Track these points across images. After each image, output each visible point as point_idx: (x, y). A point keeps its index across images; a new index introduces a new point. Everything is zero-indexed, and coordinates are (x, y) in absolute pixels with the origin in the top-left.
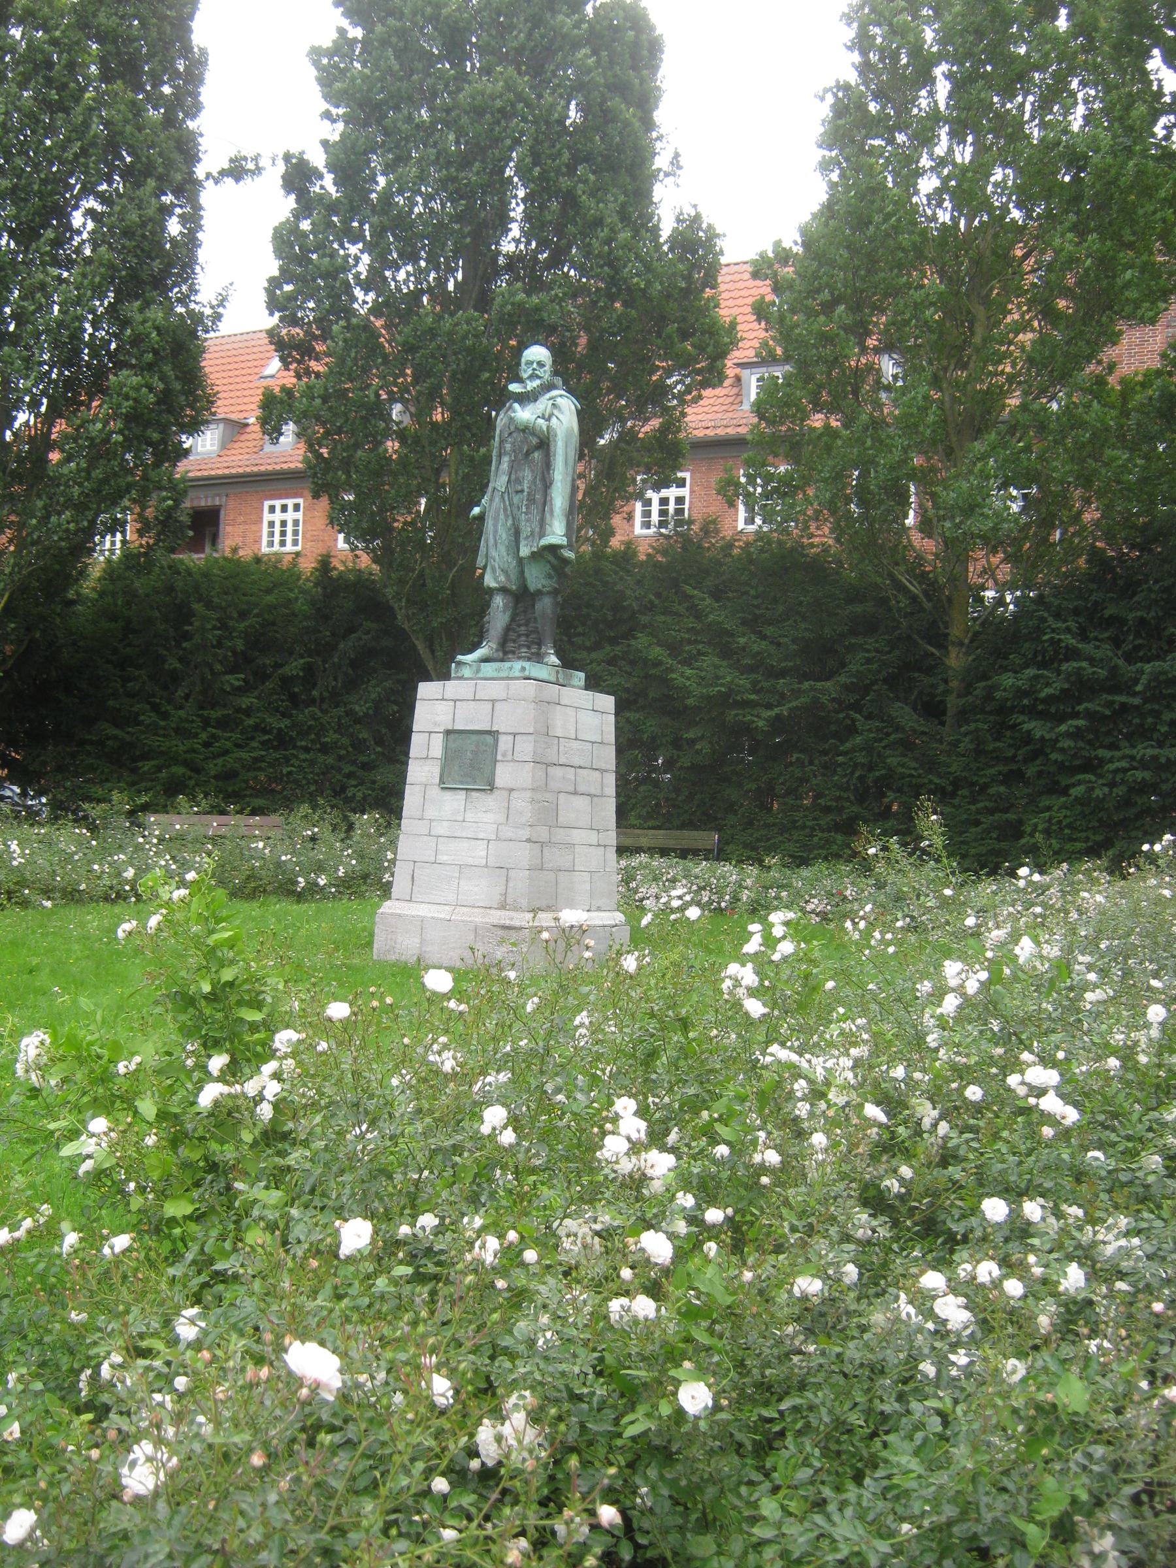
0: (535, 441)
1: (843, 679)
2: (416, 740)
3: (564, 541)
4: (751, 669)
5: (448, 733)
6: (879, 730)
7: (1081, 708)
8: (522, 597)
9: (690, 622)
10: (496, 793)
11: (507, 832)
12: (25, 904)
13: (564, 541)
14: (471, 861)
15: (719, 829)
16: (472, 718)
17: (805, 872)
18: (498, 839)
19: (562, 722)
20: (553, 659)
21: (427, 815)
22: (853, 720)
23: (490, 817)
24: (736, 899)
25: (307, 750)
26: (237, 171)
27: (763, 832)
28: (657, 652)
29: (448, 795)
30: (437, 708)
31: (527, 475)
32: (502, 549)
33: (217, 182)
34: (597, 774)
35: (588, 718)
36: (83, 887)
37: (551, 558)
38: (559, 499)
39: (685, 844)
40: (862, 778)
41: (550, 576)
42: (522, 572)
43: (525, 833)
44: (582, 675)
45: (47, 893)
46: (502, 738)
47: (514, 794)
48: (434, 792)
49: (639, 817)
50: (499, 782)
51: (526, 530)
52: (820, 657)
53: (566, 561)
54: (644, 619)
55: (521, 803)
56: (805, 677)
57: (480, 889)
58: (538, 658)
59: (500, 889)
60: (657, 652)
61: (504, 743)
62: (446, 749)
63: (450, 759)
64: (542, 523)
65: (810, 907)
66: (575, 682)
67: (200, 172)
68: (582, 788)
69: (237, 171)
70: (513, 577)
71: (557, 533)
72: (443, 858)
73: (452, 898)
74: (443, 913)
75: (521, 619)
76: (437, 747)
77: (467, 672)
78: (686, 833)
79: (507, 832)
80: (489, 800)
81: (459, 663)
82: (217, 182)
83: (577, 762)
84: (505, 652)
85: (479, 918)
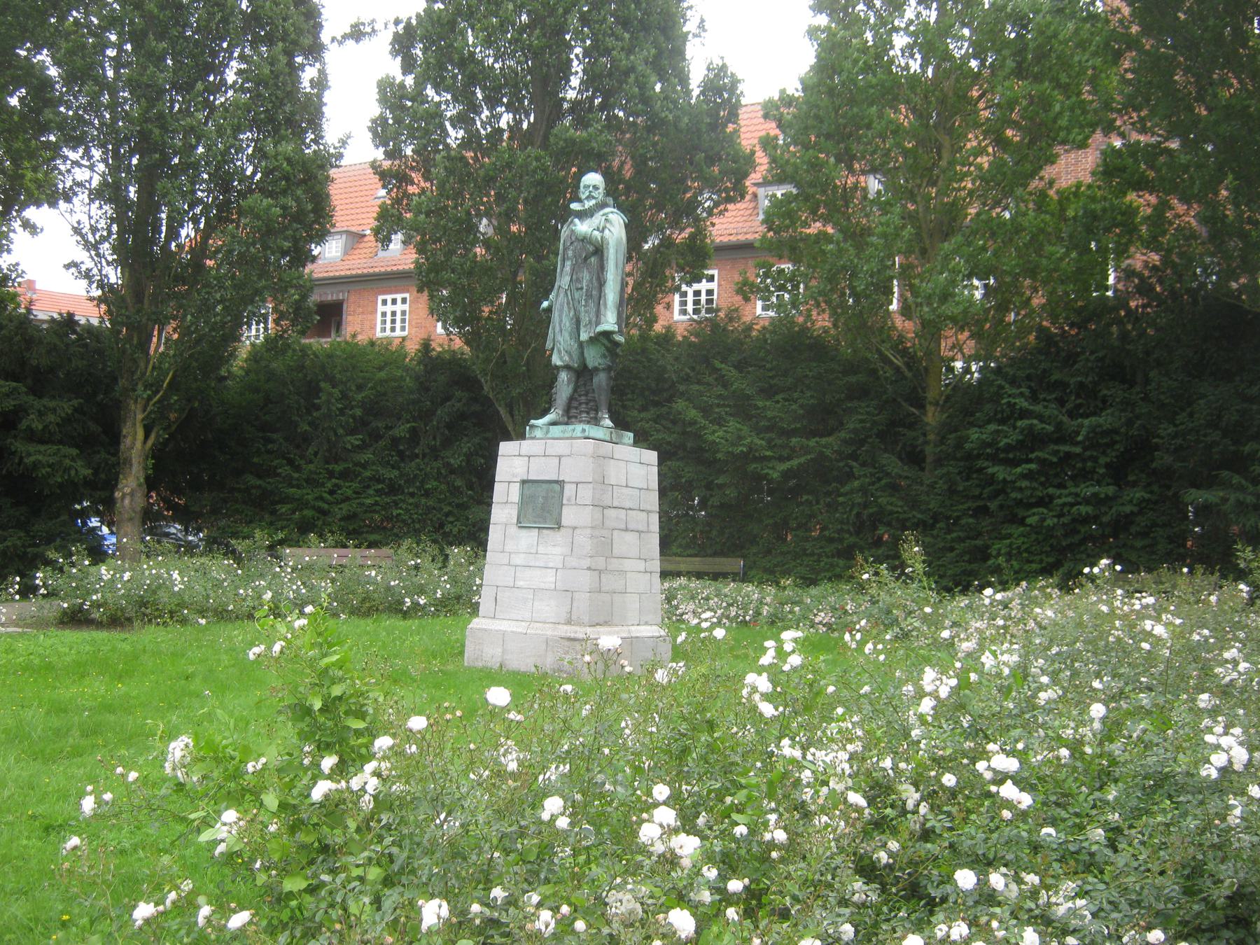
0: (591, 249)
1: (843, 435)
2: (499, 490)
3: (616, 328)
4: (769, 429)
5: (524, 482)
6: (872, 475)
7: (1032, 456)
8: (582, 373)
9: (719, 390)
11: (573, 562)
12: (184, 621)
13: (616, 328)
14: (542, 586)
15: (744, 557)
16: (543, 470)
17: (814, 591)
18: (564, 567)
19: (615, 473)
20: (608, 423)
21: (507, 548)
22: (851, 468)
23: (558, 550)
24: (758, 613)
25: (412, 495)
26: (357, 33)
27: (779, 559)
28: (693, 413)
29: (524, 533)
30: (515, 462)
31: (586, 276)
32: (566, 335)
33: (340, 43)
34: (645, 514)
35: (637, 468)
36: (231, 607)
37: (606, 342)
38: (611, 294)
39: (717, 569)
40: (858, 515)
41: (604, 356)
42: (582, 353)
43: (586, 563)
44: (631, 435)
45: (202, 612)
46: (567, 487)
47: (578, 532)
48: (513, 530)
49: (680, 546)
50: (563, 523)
51: (585, 319)
52: (822, 419)
53: (617, 344)
54: (682, 388)
55: (583, 539)
56: (814, 434)
57: (549, 609)
58: (596, 421)
60: (693, 413)
61: (569, 490)
62: (522, 495)
63: (525, 502)
64: (598, 314)
65: (817, 620)
66: (626, 440)
67: (325, 37)
68: (631, 526)
69: (357, 33)
70: (575, 357)
71: (609, 322)
72: (520, 583)
73: (527, 615)
74: (520, 628)
75: (582, 390)
76: (515, 493)
77: (538, 433)
78: (717, 560)
79: (573, 562)
80: (558, 537)
81: (532, 427)
82: (340, 43)
83: (628, 505)
84: (569, 416)
85: (549, 631)
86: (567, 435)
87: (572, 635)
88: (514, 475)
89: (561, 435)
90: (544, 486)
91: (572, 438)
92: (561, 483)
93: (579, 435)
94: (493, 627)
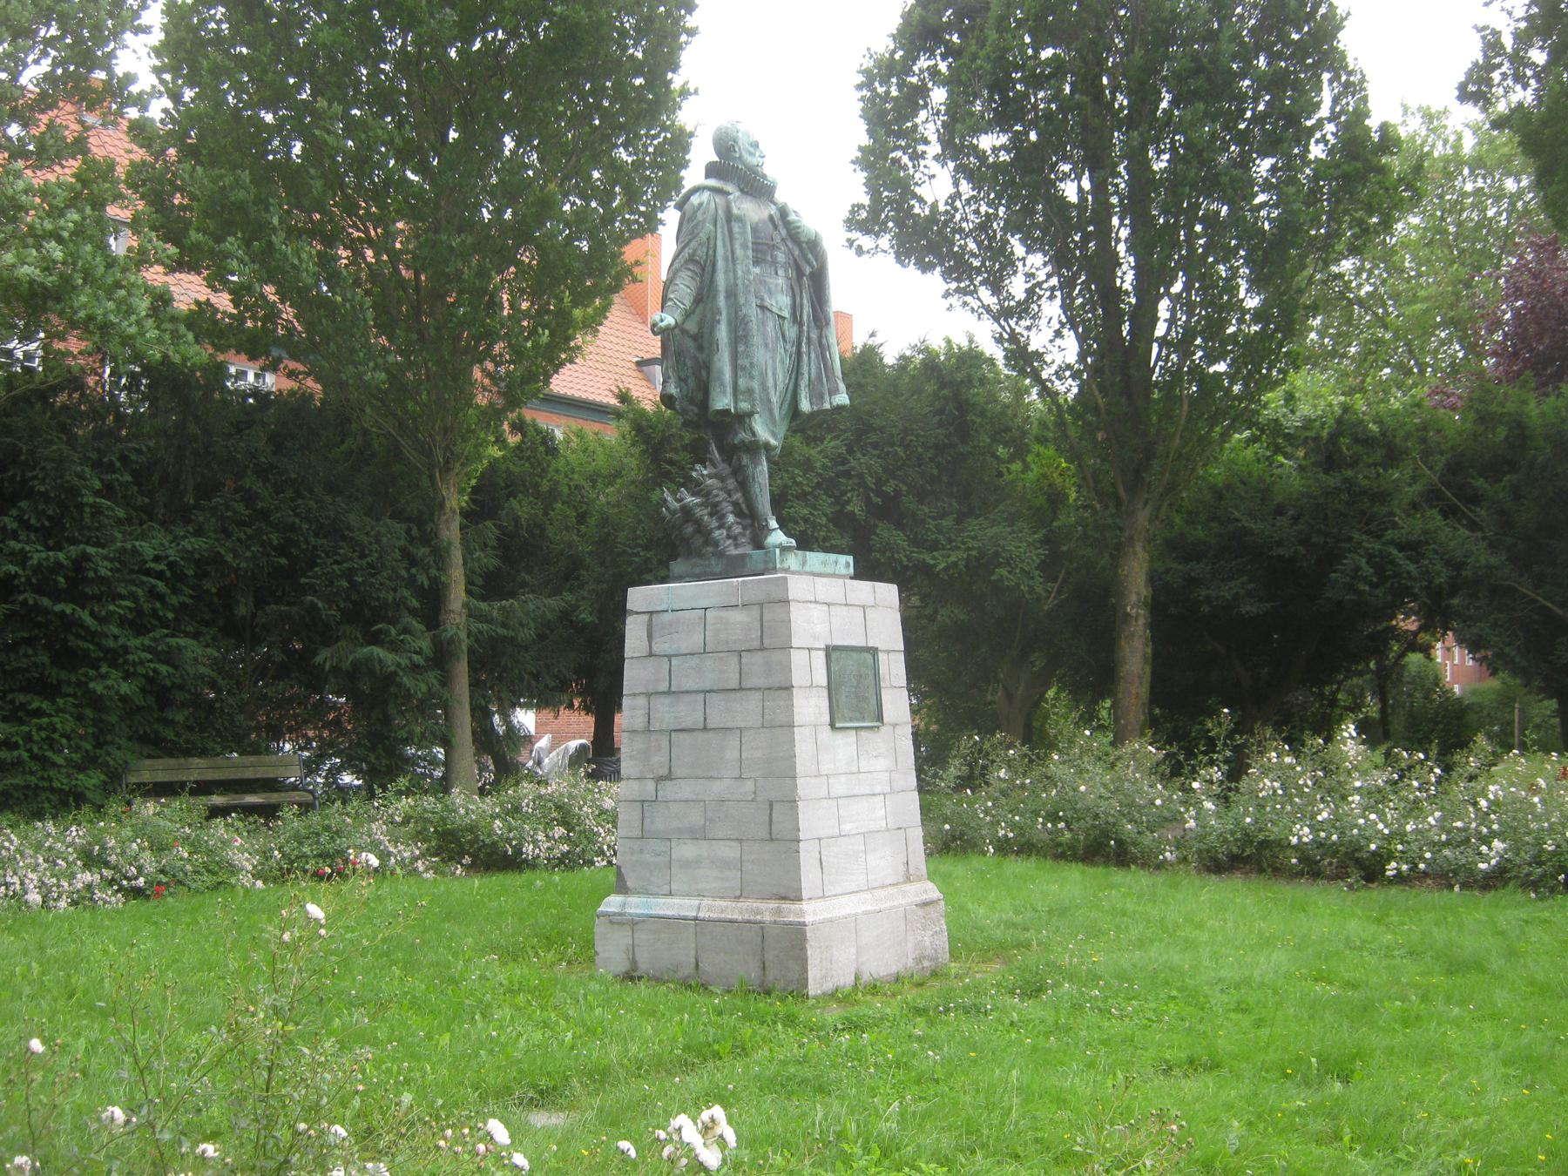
5: (830, 651)
10: (883, 729)
21: (824, 769)
46: (882, 657)
48: (826, 732)
59: (902, 858)
72: (847, 827)
86: (830, 570)
87: (924, 897)
88: (816, 638)
89: (821, 569)
90: (855, 655)
91: (833, 575)
92: (874, 651)
93: (844, 571)
94: (836, 914)
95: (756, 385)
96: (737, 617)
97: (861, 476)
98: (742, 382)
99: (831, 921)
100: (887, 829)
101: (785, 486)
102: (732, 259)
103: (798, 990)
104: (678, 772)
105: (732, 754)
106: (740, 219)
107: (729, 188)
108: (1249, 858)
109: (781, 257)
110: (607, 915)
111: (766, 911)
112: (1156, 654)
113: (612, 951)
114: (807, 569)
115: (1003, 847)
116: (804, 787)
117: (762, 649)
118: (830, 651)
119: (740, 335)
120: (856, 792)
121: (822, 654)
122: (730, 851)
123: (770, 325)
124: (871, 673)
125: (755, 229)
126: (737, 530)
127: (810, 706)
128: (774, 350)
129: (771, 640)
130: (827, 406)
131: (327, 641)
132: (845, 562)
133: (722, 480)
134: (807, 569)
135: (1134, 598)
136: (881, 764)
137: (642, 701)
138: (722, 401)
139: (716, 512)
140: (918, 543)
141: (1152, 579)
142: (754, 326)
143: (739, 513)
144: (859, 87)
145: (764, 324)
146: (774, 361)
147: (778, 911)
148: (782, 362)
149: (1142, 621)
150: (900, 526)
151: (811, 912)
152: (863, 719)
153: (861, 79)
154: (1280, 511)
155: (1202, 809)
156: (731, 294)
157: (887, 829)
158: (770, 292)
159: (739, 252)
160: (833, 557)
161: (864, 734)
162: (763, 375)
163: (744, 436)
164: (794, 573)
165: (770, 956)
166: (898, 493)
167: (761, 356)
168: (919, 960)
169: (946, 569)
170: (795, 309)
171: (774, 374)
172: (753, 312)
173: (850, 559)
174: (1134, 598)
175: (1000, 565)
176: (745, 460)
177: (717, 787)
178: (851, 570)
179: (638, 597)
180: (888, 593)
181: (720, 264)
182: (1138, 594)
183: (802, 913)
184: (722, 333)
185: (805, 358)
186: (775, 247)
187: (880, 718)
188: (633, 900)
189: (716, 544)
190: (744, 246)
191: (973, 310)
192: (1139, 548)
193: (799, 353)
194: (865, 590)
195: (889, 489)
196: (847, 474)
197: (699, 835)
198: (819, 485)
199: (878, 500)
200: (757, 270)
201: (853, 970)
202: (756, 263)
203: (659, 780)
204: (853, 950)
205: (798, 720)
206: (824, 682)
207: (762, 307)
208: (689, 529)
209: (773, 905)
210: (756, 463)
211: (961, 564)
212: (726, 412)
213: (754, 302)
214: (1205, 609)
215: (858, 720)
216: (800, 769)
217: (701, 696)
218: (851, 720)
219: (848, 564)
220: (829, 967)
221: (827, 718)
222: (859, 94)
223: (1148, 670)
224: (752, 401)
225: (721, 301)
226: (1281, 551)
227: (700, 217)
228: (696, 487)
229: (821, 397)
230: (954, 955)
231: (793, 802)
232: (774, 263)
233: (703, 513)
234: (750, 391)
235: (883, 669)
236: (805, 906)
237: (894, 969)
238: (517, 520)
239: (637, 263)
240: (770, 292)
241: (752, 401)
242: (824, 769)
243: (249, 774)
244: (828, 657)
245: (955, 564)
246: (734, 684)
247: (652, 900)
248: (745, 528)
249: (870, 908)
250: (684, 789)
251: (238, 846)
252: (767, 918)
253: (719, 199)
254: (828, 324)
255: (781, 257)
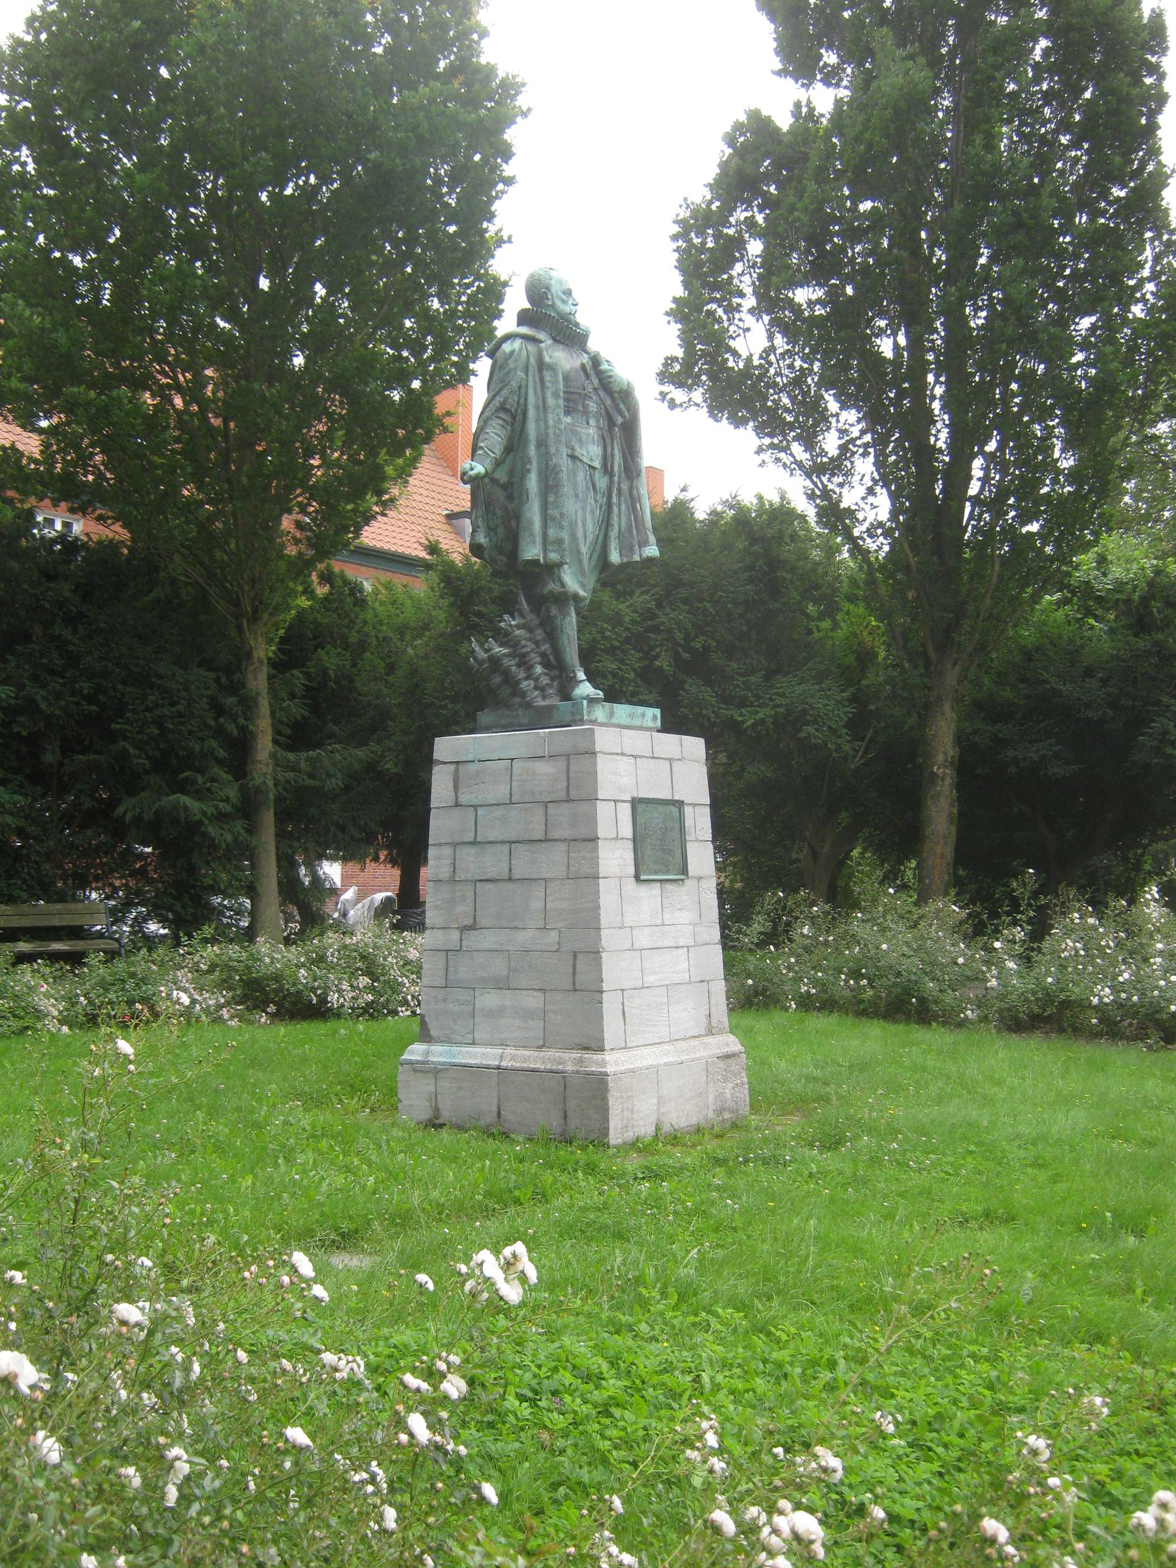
5: (636, 803)
10: (688, 882)
14: (676, 978)
46: (688, 810)
48: (630, 885)
50: (692, 870)
57: (687, 1014)
72: (650, 979)
80: (683, 894)
86: (637, 723)
87: (726, 1050)
89: (628, 721)
90: (661, 808)
92: (680, 804)
93: (650, 724)
94: (638, 1064)
95: (565, 535)
96: (543, 768)
97: (669, 631)
98: (552, 532)
99: (633, 1071)
100: (690, 982)
101: (594, 640)
102: (543, 408)
103: (599, 1140)
104: (483, 921)
105: (536, 905)
106: (552, 368)
107: (541, 336)
108: (1050, 1017)
109: (592, 406)
110: (410, 1062)
111: (567, 1060)
112: (962, 815)
113: (415, 1099)
114: (614, 721)
115: (806, 1004)
116: (609, 938)
117: (569, 800)
118: (636, 803)
119: (550, 486)
120: (659, 944)
121: (628, 806)
122: (532, 1001)
123: (581, 476)
124: (677, 826)
125: (566, 378)
126: (545, 681)
127: (615, 858)
128: (584, 501)
129: (578, 792)
130: (636, 558)
131: (132, 792)
132: (652, 715)
133: (531, 630)
134: (614, 721)
135: (941, 758)
136: (686, 917)
137: (447, 851)
138: (531, 551)
139: (524, 662)
140: (726, 699)
141: (959, 739)
142: (564, 476)
143: (546, 664)
144: (675, 238)
145: (574, 475)
146: (584, 512)
147: (580, 1061)
148: (592, 512)
149: (948, 781)
150: (708, 682)
151: (613, 1062)
152: (668, 872)
153: (676, 229)
154: (1089, 672)
155: (1004, 968)
156: (542, 443)
157: (690, 982)
158: (581, 441)
159: (551, 401)
160: (640, 709)
161: (669, 886)
162: (573, 526)
163: (552, 586)
164: (602, 725)
165: (572, 1105)
166: (706, 649)
167: (571, 506)
168: (719, 1112)
169: (753, 726)
170: (606, 459)
171: (584, 524)
172: (564, 462)
173: (658, 712)
174: (941, 758)
175: (807, 723)
176: (554, 611)
177: (522, 938)
178: (659, 723)
179: (445, 747)
180: (695, 746)
181: (531, 413)
182: (945, 754)
183: (604, 1063)
184: (533, 483)
185: (615, 509)
186: (587, 397)
187: (684, 870)
188: (437, 1048)
189: (523, 695)
190: (556, 395)
191: (785, 465)
192: (947, 707)
193: (609, 504)
194: (671, 743)
195: (697, 644)
196: (656, 629)
197: (502, 984)
198: (628, 639)
199: (686, 656)
200: (568, 420)
201: (654, 1119)
202: (568, 412)
203: (464, 929)
204: (654, 1101)
205: (603, 871)
206: (630, 836)
207: (573, 457)
208: (497, 680)
209: (576, 1055)
210: (565, 614)
211: (769, 721)
212: (535, 562)
213: (564, 451)
214: (1013, 770)
215: (662, 873)
216: (604, 920)
217: (506, 848)
218: (656, 873)
219: (655, 717)
220: (632, 1116)
221: (632, 870)
222: (674, 245)
223: (953, 829)
224: (561, 551)
225: (532, 450)
226: (1090, 714)
227: (511, 365)
228: (503, 637)
229: (631, 550)
230: (754, 1107)
231: (596, 954)
232: (586, 412)
233: (510, 664)
234: (560, 542)
235: (689, 822)
236: (608, 1056)
237: (694, 1121)
238: (325, 671)
239: (448, 414)
240: (581, 441)
241: (561, 551)
242: (629, 920)
243: (55, 922)
244: (634, 809)
245: (762, 721)
246: (539, 835)
247: (455, 1049)
248: (552, 679)
249: (671, 1059)
250: (486, 939)
251: (44, 991)
252: (570, 1067)
253: (531, 347)
254: (639, 475)
255: (592, 406)
